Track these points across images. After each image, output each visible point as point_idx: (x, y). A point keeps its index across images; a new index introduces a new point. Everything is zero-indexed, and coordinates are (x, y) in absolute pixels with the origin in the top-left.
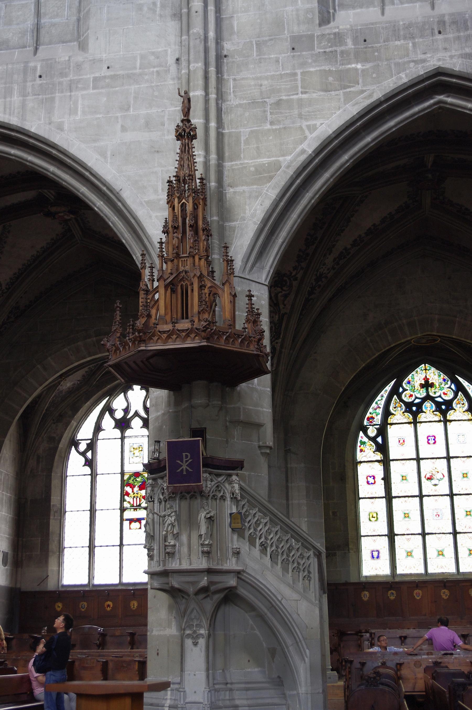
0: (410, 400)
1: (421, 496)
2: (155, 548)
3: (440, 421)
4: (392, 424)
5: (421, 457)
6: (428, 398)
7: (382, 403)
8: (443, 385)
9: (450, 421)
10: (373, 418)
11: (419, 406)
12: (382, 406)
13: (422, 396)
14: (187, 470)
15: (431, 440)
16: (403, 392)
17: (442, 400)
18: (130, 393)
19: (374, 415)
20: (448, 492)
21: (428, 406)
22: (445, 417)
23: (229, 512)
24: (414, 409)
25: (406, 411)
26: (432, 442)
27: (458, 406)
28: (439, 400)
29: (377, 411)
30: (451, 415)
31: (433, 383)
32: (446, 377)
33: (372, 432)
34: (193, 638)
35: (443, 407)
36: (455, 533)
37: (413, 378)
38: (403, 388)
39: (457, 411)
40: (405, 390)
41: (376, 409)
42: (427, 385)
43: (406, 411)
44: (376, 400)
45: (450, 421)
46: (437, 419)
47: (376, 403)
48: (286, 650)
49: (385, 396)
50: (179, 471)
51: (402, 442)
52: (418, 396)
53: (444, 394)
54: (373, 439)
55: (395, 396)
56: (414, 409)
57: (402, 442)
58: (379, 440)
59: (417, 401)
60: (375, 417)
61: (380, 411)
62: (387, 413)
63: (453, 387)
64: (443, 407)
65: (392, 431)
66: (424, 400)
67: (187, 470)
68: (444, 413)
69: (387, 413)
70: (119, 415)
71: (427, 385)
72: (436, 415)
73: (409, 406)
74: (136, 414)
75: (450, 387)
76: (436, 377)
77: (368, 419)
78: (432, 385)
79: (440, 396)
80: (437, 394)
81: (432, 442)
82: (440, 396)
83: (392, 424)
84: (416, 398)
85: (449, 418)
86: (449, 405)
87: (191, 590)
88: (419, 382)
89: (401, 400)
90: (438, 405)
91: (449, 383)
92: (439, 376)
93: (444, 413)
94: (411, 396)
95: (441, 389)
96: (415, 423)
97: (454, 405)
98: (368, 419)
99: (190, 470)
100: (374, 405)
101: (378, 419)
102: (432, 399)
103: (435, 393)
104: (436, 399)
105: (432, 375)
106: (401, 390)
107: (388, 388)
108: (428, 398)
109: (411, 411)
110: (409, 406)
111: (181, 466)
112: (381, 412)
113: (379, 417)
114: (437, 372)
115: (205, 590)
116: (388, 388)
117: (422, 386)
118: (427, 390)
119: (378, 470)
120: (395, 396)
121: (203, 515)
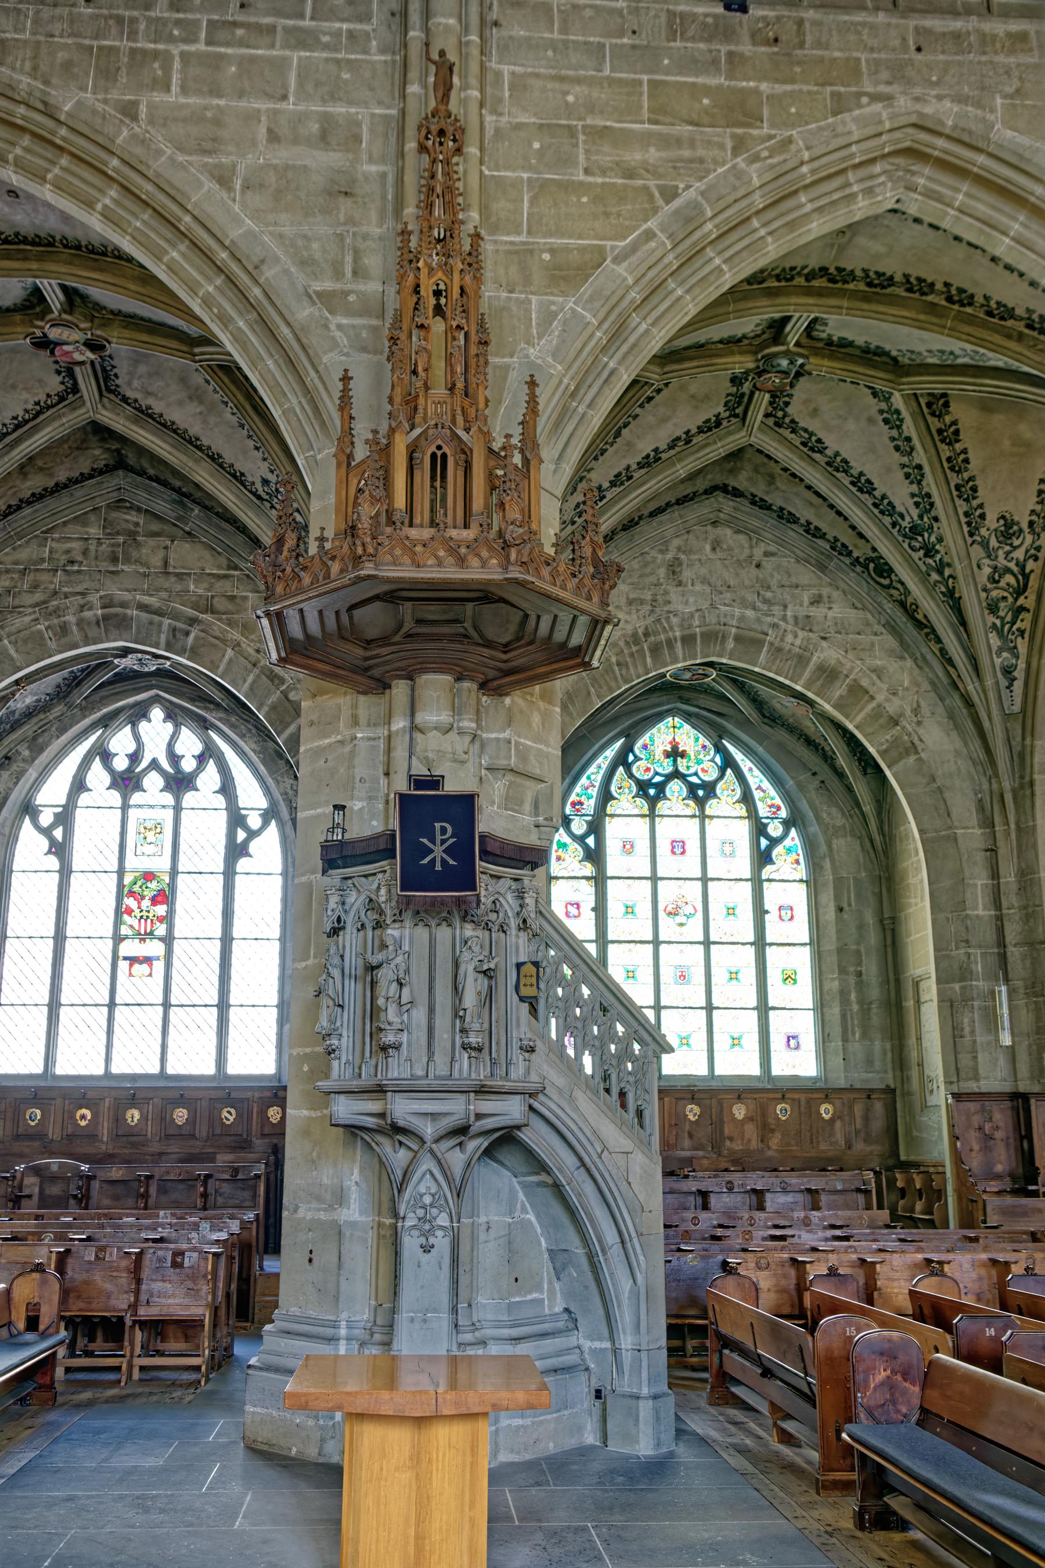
0: (646, 777)
1: (656, 942)
2: (345, 1034)
3: (694, 816)
4: (612, 816)
5: (659, 875)
6: (676, 774)
7: (598, 779)
8: (701, 756)
9: (711, 817)
10: (581, 803)
11: (661, 787)
12: (597, 784)
13: (666, 772)
14: (444, 862)
15: (678, 847)
16: (634, 762)
17: (699, 782)
18: (143, 726)
19: (583, 799)
20: (700, 938)
21: (675, 788)
22: (702, 809)
23: (514, 961)
24: (652, 792)
25: (637, 796)
26: (678, 851)
27: (726, 793)
28: (694, 780)
29: (590, 791)
30: (712, 807)
31: (684, 751)
32: (707, 743)
33: (579, 826)
34: (425, 1234)
35: (701, 793)
36: (710, 1008)
37: (652, 740)
38: (635, 756)
39: (723, 801)
40: (637, 759)
41: (587, 789)
42: (675, 753)
43: (637, 796)
44: (588, 773)
45: (711, 817)
46: (689, 812)
47: (588, 778)
48: (601, 1258)
49: (604, 767)
50: (425, 861)
51: (628, 847)
52: (660, 770)
53: (703, 770)
54: (581, 839)
55: (621, 768)
56: (652, 792)
57: (628, 847)
58: (591, 841)
59: (658, 779)
60: (586, 803)
61: (594, 792)
62: (606, 796)
63: (718, 759)
64: (701, 793)
65: (614, 830)
66: (669, 777)
67: (444, 862)
68: (701, 803)
69: (606, 796)
70: (121, 764)
71: (675, 753)
72: (687, 805)
73: (642, 786)
74: (154, 764)
75: (712, 760)
76: (692, 741)
77: (573, 804)
78: (683, 754)
79: (696, 774)
80: (692, 771)
81: (678, 851)
82: (696, 774)
83: (612, 816)
84: (657, 774)
85: (708, 812)
86: (710, 789)
87: (429, 1130)
88: (662, 748)
89: (631, 776)
90: (692, 788)
91: (712, 752)
92: (697, 740)
93: (701, 803)
94: (648, 770)
95: (699, 762)
96: (652, 815)
97: (718, 791)
98: (573, 804)
99: (452, 862)
100: (584, 781)
101: (590, 805)
102: (683, 777)
103: (688, 767)
104: (689, 779)
105: (684, 737)
106: (631, 758)
107: (610, 753)
108: (676, 774)
109: (646, 796)
110: (642, 786)
111: (432, 851)
112: (595, 794)
113: (592, 802)
114: (693, 732)
115: (461, 1131)
116: (610, 753)
117: (667, 755)
118: (675, 761)
119: (586, 894)
120: (621, 768)
121: (470, 968)
